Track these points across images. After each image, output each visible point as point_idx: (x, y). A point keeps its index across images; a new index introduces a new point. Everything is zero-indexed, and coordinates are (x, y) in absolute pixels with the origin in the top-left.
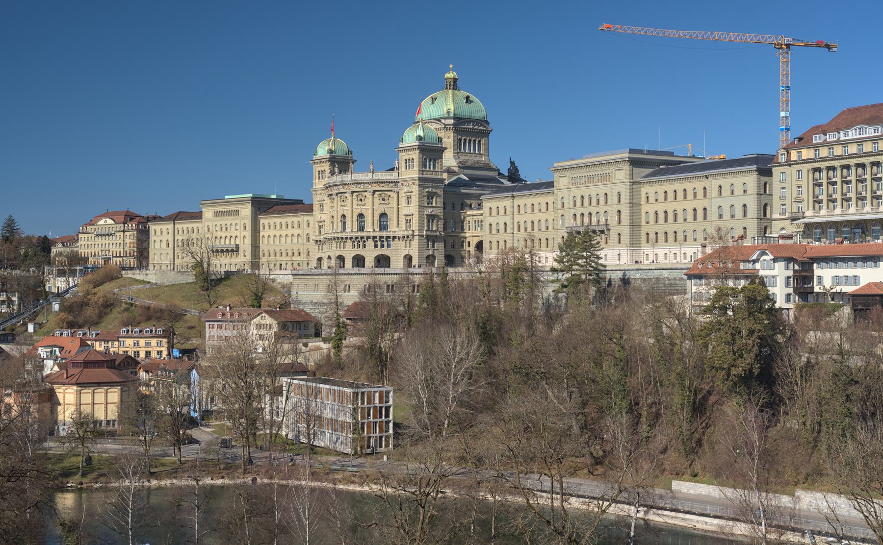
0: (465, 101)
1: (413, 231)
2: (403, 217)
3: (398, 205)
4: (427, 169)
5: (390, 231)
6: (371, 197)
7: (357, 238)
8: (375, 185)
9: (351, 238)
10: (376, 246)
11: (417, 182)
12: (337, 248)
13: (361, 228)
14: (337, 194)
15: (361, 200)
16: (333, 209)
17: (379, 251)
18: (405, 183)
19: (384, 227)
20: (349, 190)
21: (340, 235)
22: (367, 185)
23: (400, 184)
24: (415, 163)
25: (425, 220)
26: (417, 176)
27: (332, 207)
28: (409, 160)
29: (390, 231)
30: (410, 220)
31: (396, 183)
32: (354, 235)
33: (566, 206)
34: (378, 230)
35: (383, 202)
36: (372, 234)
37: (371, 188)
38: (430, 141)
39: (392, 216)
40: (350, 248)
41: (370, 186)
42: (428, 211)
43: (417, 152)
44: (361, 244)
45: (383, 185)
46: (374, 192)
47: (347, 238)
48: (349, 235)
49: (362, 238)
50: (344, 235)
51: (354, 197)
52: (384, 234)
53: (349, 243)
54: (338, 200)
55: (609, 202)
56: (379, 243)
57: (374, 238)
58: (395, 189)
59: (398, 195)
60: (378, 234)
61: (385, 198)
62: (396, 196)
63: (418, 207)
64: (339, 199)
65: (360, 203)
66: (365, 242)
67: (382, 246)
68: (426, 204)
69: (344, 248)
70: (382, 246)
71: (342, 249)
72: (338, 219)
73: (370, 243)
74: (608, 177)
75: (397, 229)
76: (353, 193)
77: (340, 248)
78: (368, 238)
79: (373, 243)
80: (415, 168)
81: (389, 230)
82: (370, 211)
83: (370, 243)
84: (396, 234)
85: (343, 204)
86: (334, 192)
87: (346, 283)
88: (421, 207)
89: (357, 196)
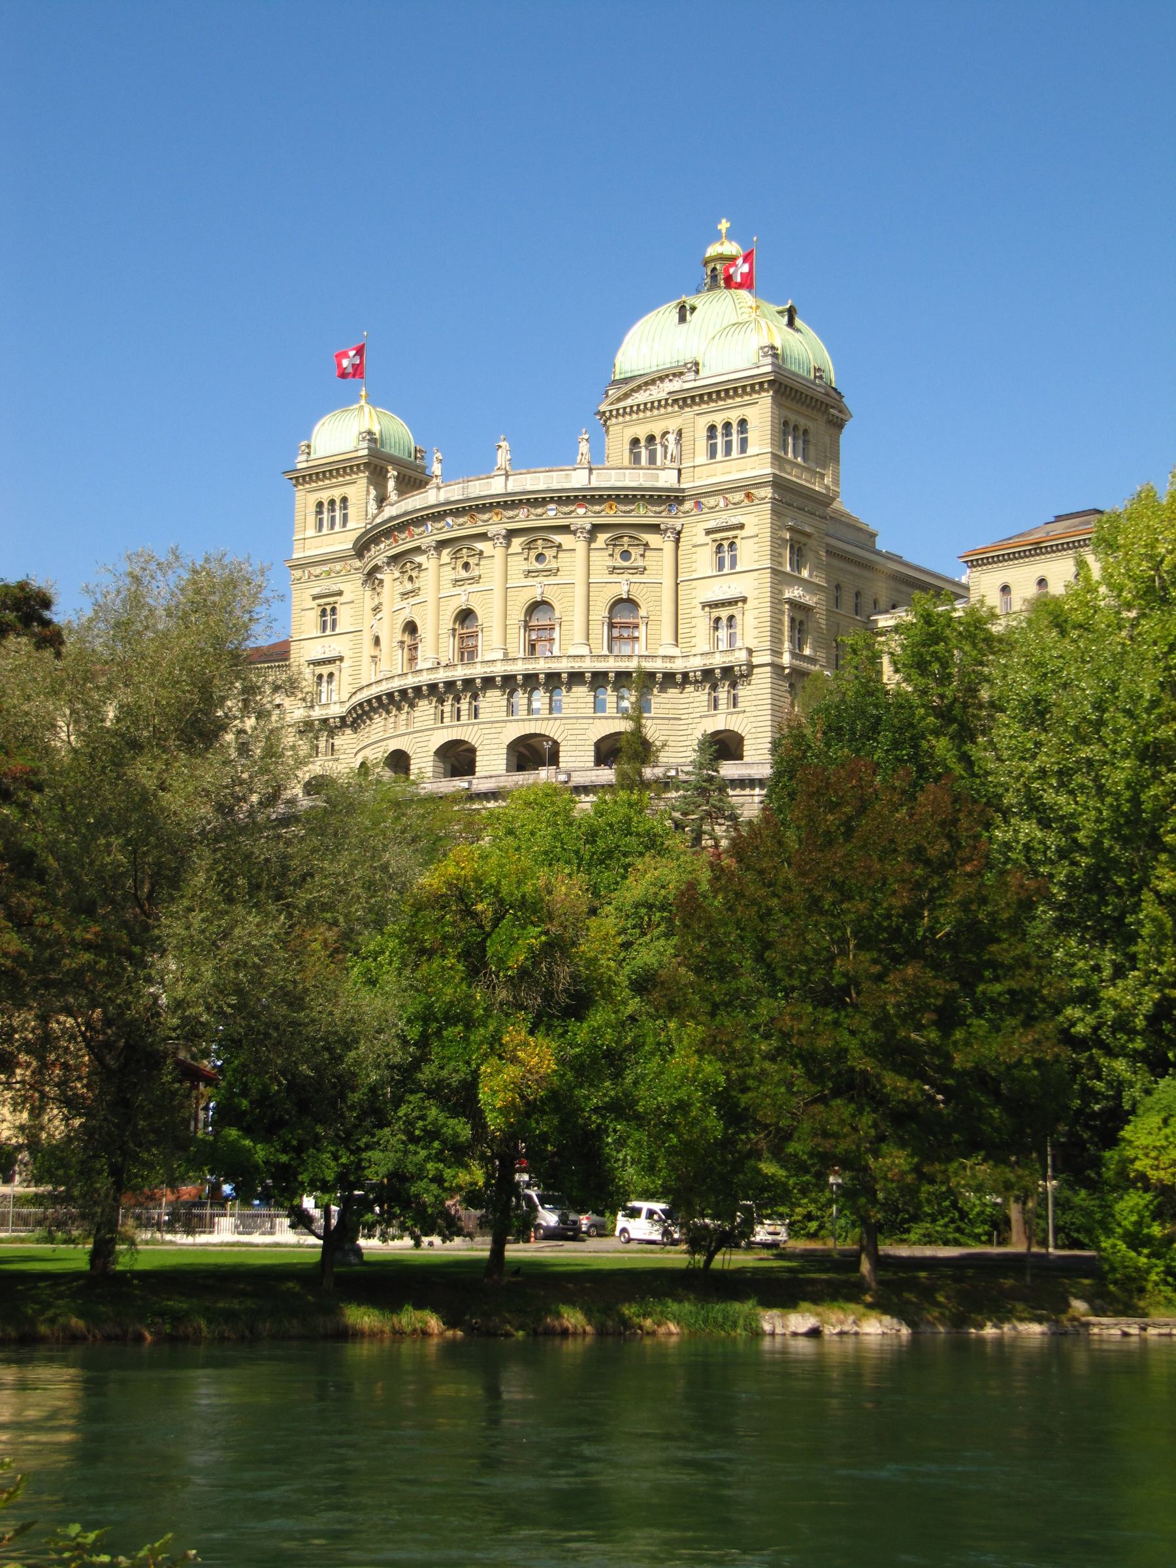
0: (785, 319)
1: (750, 651)
2: (698, 611)
4: (790, 455)
6: (580, 546)
11: (767, 492)
15: (540, 557)
18: (711, 501)
20: (496, 525)
23: (688, 505)
24: (752, 435)
25: (786, 619)
26: (769, 471)
28: (727, 425)
30: (731, 618)
31: (672, 499)
37: (582, 517)
38: (794, 368)
41: (581, 511)
42: (793, 592)
43: (765, 400)
46: (596, 529)
47: (488, 682)
53: (493, 701)
59: (677, 541)
61: (632, 550)
62: (669, 546)
63: (767, 575)
68: (788, 569)
80: (751, 450)
82: (580, 590)
84: (678, 666)
88: (779, 577)
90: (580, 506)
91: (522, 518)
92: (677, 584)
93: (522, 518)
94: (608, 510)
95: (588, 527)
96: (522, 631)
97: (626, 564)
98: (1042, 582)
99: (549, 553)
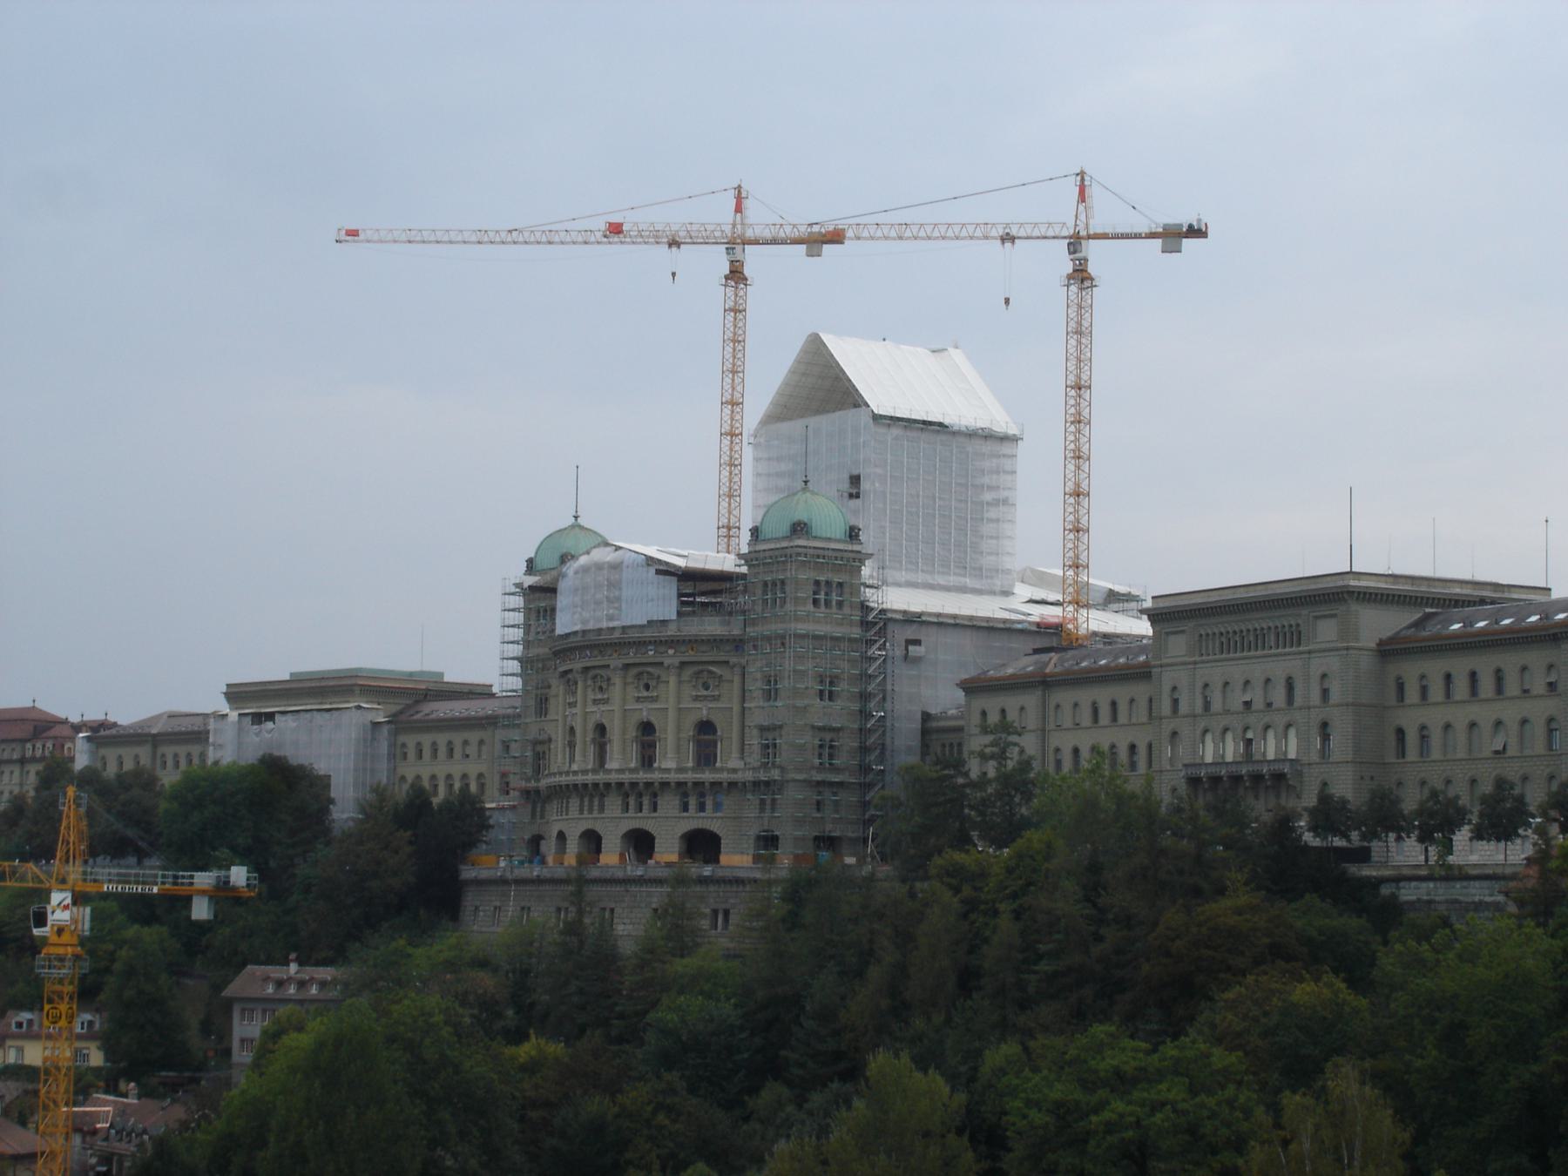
2: (755, 732)
3: (743, 700)
5: (721, 770)
6: (673, 680)
7: (634, 785)
8: (683, 649)
9: (620, 785)
10: (685, 808)
12: (581, 811)
13: (647, 761)
14: (586, 669)
15: (647, 687)
16: (574, 711)
17: (693, 821)
19: (706, 756)
20: (615, 661)
21: (590, 778)
22: (662, 649)
27: (573, 705)
29: (721, 770)
31: (738, 644)
32: (626, 777)
33: (1184, 708)
34: (690, 764)
35: (705, 693)
36: (673, 777)
37: (671, 657)
39: (728, 733)
40: (618, 813)
41: (671, 652)
44: (646, 801)
45: (704, 648)
46: (683, 664)
47: (608, 785)
48: (614, 778)
49: (649, 785)
50: (601, 777)
51: (630, 680)
52: (707, 776)
53: (613, 804)
54: (586, 687)
55: (1298, 701)
56: (693, 802)
57: (679, 784)
58: (733, 660)
60: (689, 777)
61: (711, 682)
62: (737, 679)
64: (589, 682)
65: (645, 694)
66: (655, 795)
67: (702, 807)
69: (602, 809)
70: (702, 807)
71: (595, 814)
72: (584, 736)
73: (668, 804)
74: (1293, 637)
75: (738, 764)
76: (627, 667)
77: (591, 811)
78: (665, 785)
79: (676, 802)
81: (718, 764)
82: (672, 714)
83: (668, 804)
84: (739, 777)
85: (599, 696)
86: (577, 665)
87: (602, 905)
89: (639, 676)
90: (671, 648)
91: (632, 657)
92: (744, 708)
93: (632, 657)
94: (690, 651)
95: (677, 665)
96: (634, 745)
97: (705, 693)
98: (1003, 711)
99: (652, 683)
